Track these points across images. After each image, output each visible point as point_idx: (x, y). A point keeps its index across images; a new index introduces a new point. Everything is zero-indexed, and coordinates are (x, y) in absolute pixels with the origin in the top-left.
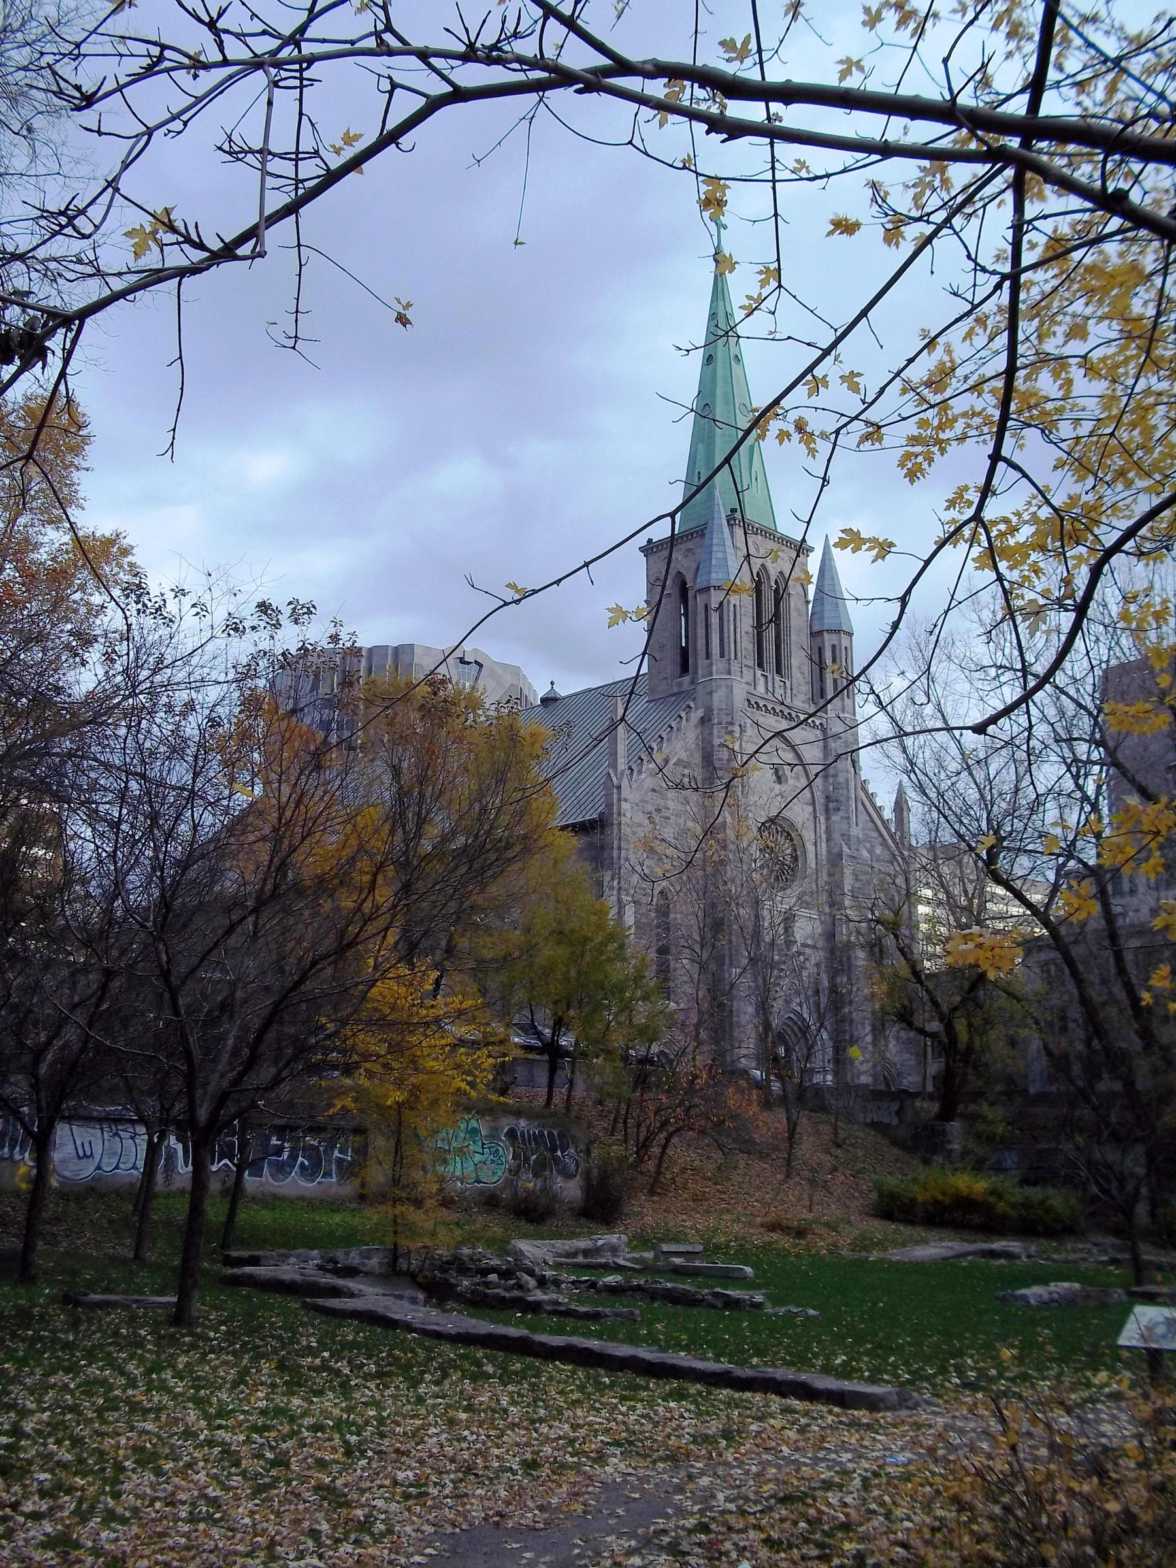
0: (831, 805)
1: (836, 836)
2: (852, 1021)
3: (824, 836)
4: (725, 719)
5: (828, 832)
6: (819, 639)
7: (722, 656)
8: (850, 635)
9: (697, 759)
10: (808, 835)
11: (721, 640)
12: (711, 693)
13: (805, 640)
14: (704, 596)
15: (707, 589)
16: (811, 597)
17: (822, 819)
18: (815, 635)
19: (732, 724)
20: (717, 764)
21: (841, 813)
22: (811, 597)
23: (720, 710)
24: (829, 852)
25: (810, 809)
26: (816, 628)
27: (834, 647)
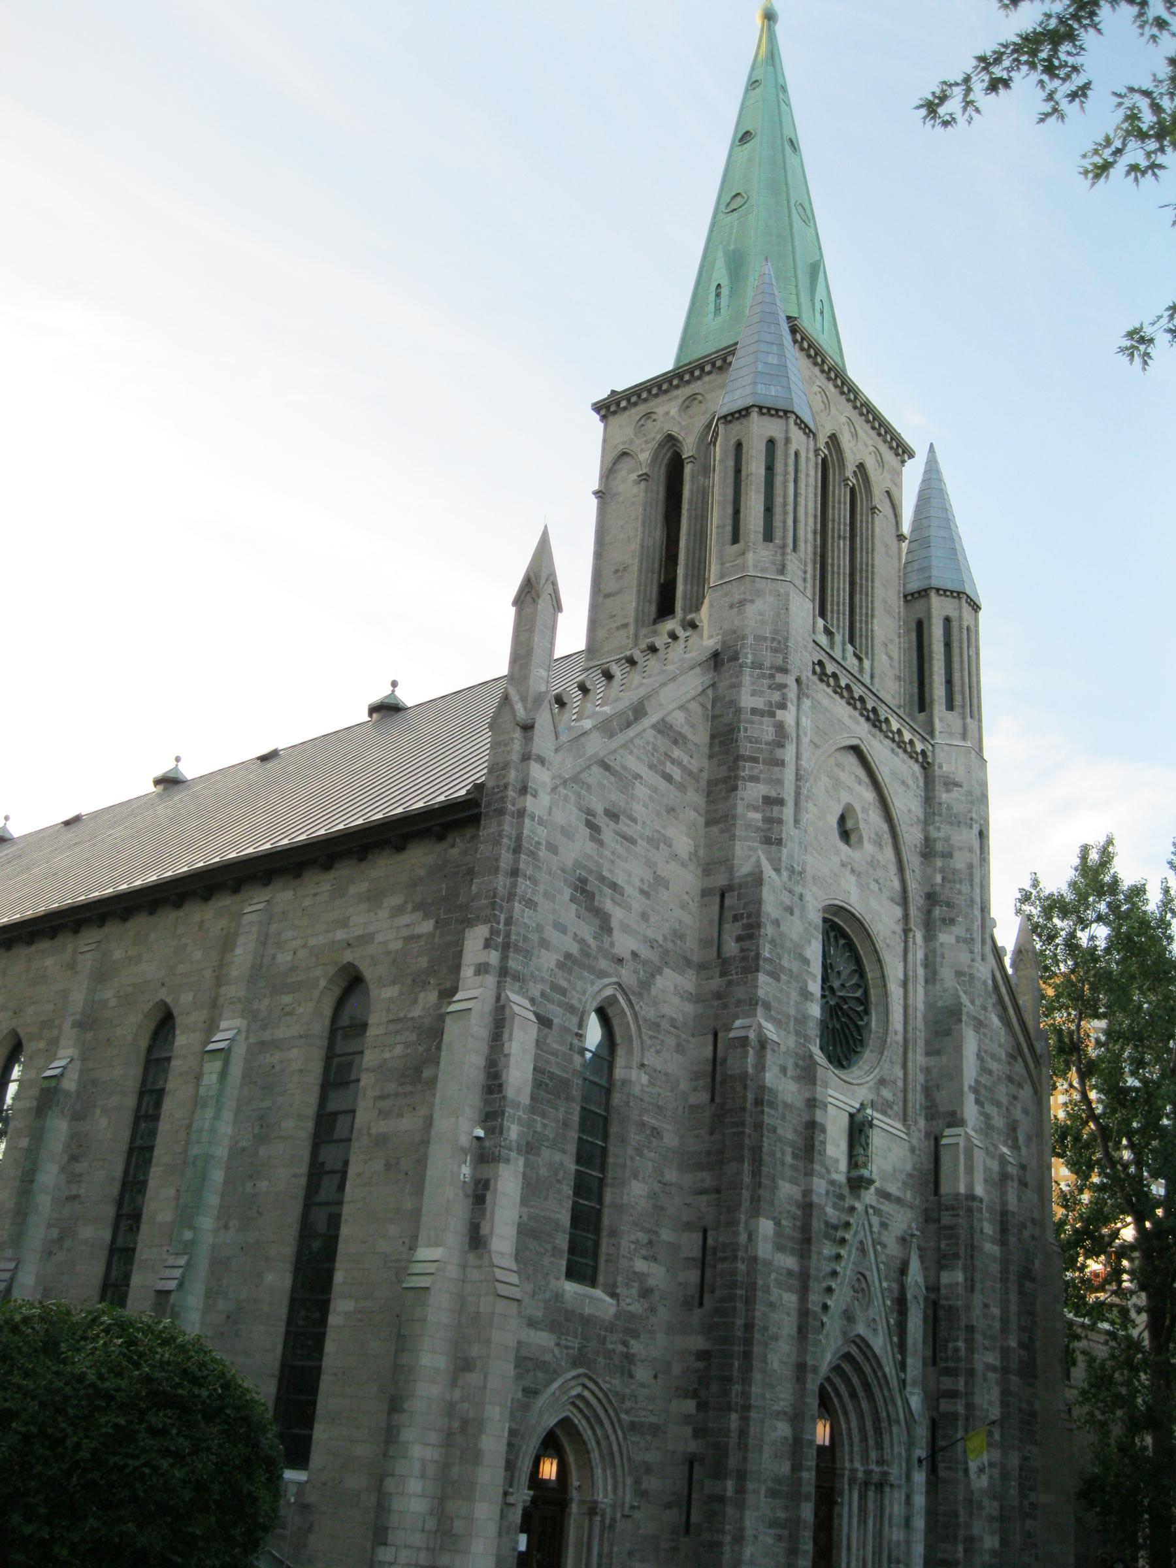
0: (937, 912)
1: (946, 974)
2: (971, 1373)
3: (921, 971)
4: (768, 659)
5: (930, 965)
6: (919, 606)
7: (768, 536)
8: (976, 607)
9: (700, 736)
10: (894, 969)
11: (769, 510)
12: (742, 603)
13: (896, 602)
14: (736, 427)
15: (743, 413)
16: (906, 529)
17: (919, 936)
18: (916, 597)
19: (784, 670)
20: (746, 749)
21: (957, 930)
22: (906, 529)
23: (759, 639)
24: (930, 1005)
25: (898, 912)
26: (913, 586)
27: (947, 620)
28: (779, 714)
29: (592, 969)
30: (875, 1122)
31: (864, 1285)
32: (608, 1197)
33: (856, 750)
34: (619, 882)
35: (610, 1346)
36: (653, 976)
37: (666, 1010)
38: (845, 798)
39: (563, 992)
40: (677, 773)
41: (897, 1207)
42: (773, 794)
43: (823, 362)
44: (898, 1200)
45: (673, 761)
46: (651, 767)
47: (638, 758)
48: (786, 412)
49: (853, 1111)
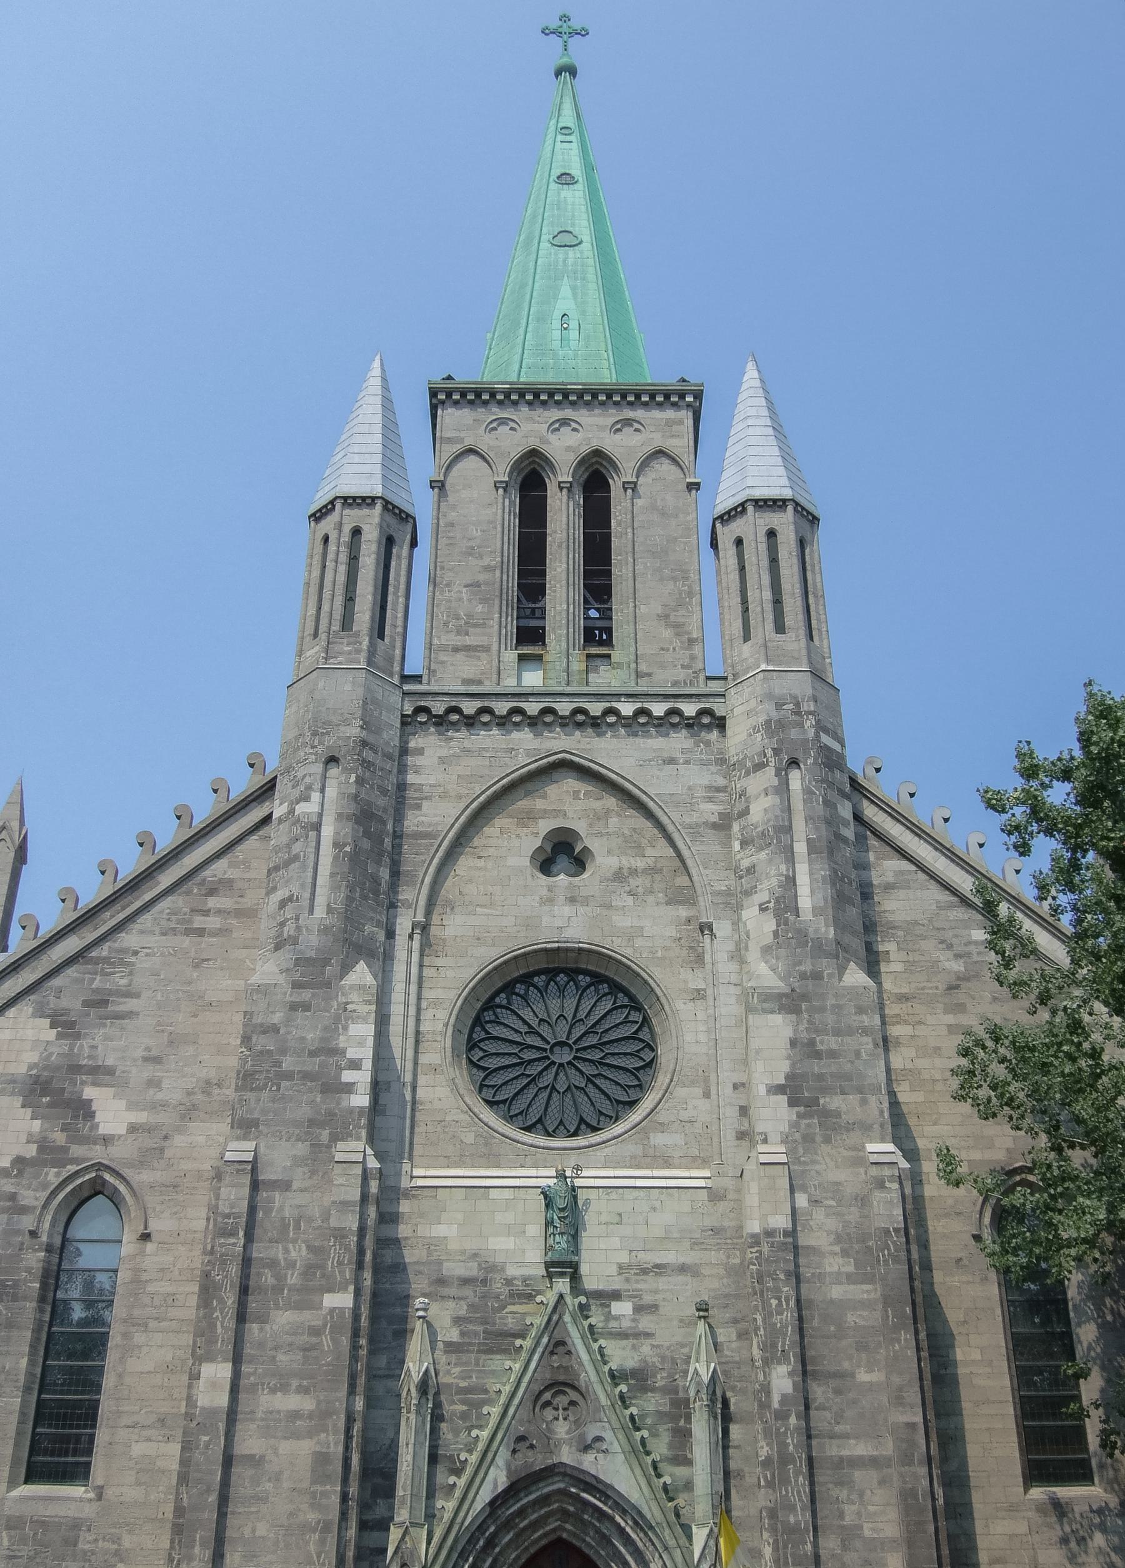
28: (301, 808)
29: (55, 1163)
30: (578, 1182)
31: (573, 1395)
32: (109, 1381)
33: (563, 766)
34: (109, 1062)
35: (87, 1547)
36: (166, 1138)
37: (186, 1166)
38: (545, 826)
39: (13, 1197)
40: (213, 922)
41: (681, 1278)
42: (287, 894)
43: (493, 395)
44: (683, 1269)
45: (206, 913)
46: (164, 934)
47: (142, 932)
48: (332, 502)
49: (552, 1182)
